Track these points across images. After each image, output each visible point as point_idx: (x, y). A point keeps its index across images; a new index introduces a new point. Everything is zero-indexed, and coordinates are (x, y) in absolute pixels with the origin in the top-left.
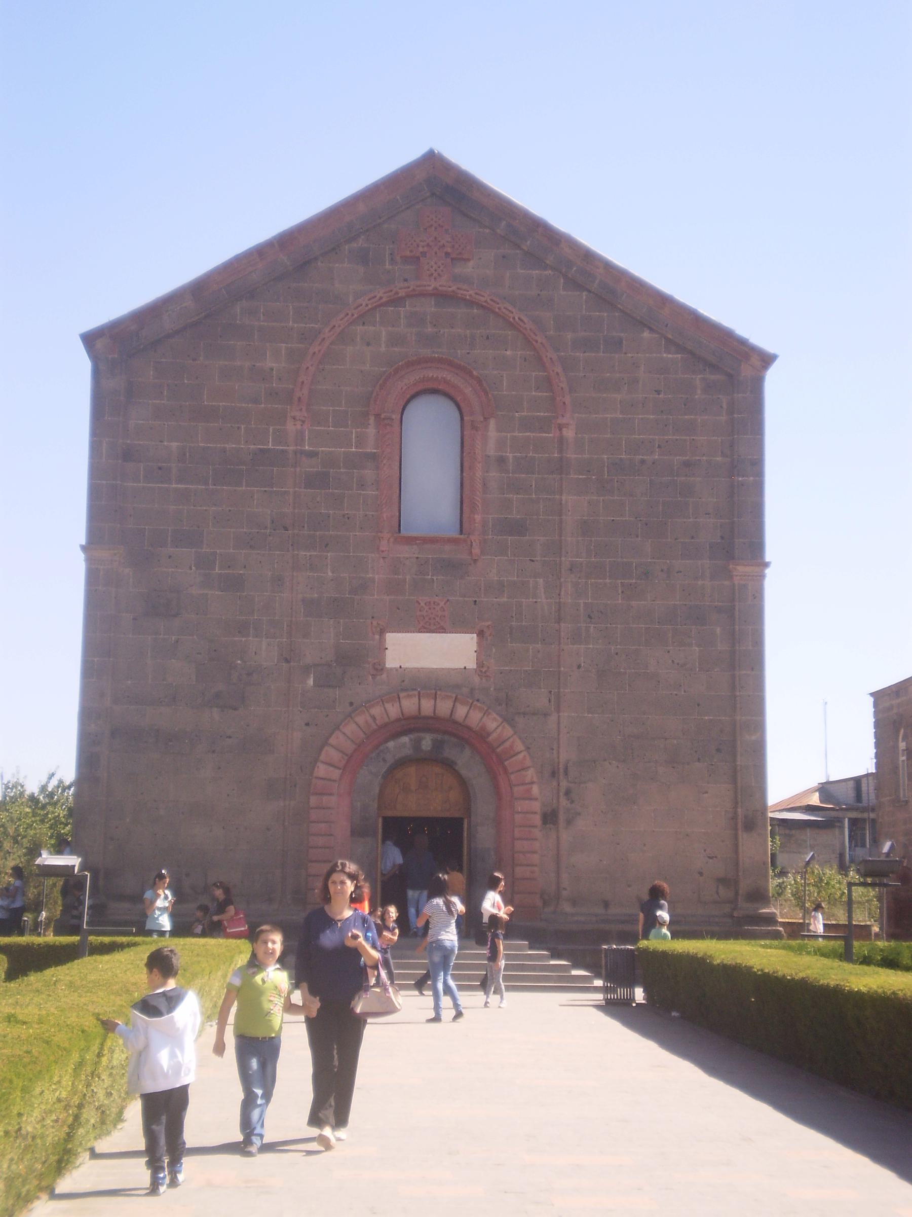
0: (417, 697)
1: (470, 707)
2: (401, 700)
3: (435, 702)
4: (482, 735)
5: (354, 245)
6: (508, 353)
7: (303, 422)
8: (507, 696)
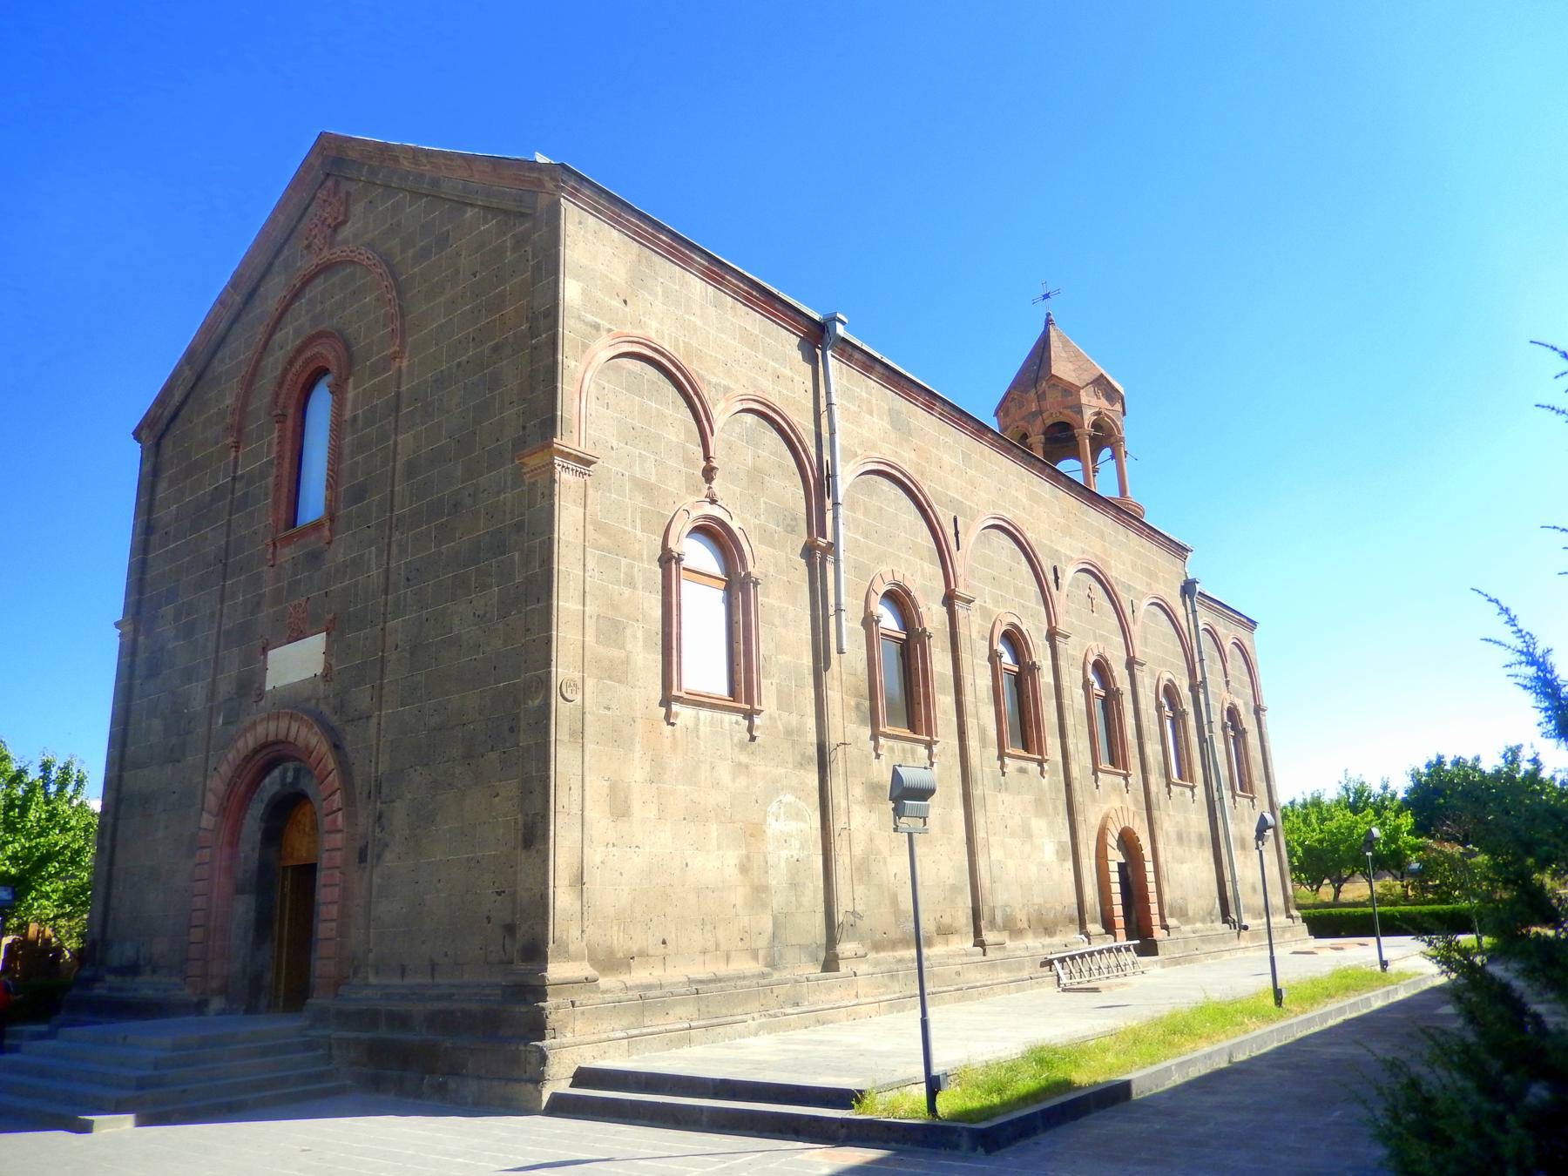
4: (309, 752)
5: (281, 258)
6: (368, 299)
7: (237, 448)
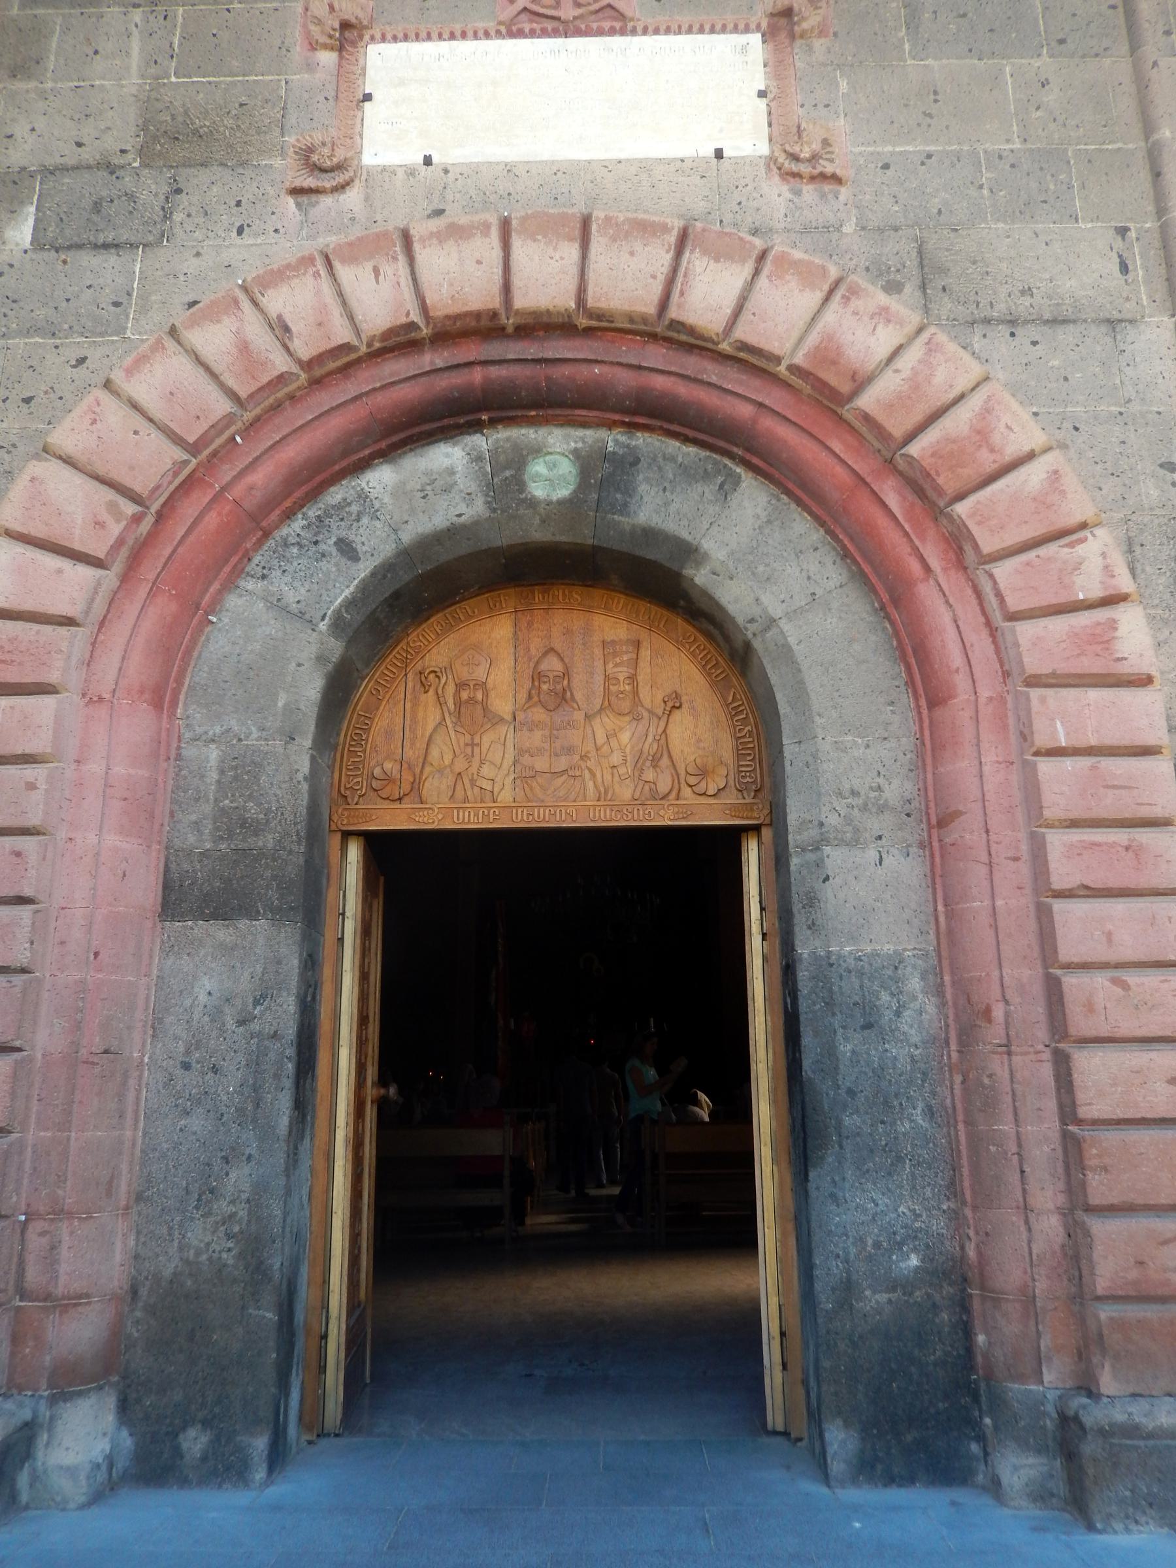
0: (495, 233)
1: (757, 272)
2: (417, 247)
3: (584, 256)
8: (920, 253)
